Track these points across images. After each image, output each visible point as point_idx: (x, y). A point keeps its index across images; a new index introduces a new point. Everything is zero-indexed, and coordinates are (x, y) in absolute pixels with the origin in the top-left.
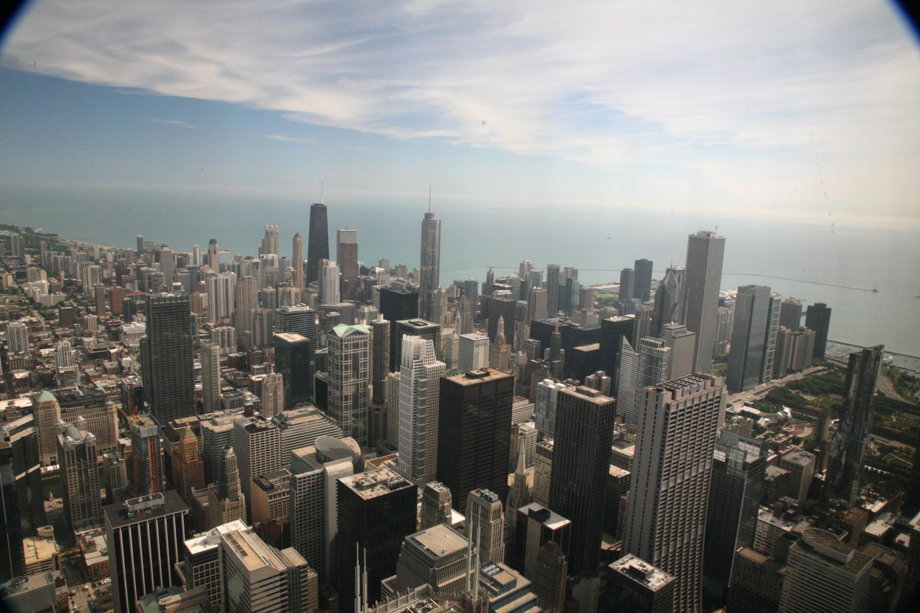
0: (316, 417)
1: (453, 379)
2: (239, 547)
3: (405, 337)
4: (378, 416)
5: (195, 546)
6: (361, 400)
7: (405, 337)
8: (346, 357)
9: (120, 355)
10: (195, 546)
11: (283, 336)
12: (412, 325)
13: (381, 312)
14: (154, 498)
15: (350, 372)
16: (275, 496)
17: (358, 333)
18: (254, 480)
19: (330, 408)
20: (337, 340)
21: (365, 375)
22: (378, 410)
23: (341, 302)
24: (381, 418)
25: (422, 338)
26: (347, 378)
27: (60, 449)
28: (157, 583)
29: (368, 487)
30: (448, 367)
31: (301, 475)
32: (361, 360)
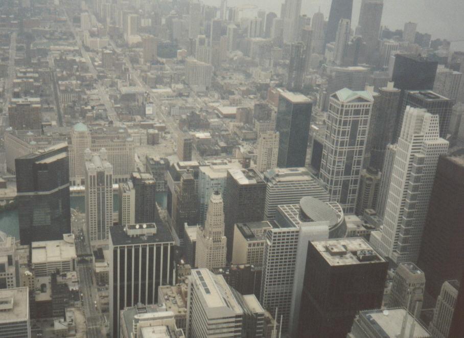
0: (306, 178)
1: (454, 159)
2: (204, 285)
3: (409, 110)
4: (369, 185)
7: (409, 110)
8: (345, 123)
12: (422, 96)
14: (148, 227)
15: (347, 138)
16: (254, 245)
17: (360, 99)
19: (322, 171)
20: (338, 105)
21: (362, 143)
22: (370, 179)
24: (373, 187)
25: (428, 111)
26: (342, 144)
28: (136, 302)
30: (452, 145)
31: (276, 230)
32: (361, 128)
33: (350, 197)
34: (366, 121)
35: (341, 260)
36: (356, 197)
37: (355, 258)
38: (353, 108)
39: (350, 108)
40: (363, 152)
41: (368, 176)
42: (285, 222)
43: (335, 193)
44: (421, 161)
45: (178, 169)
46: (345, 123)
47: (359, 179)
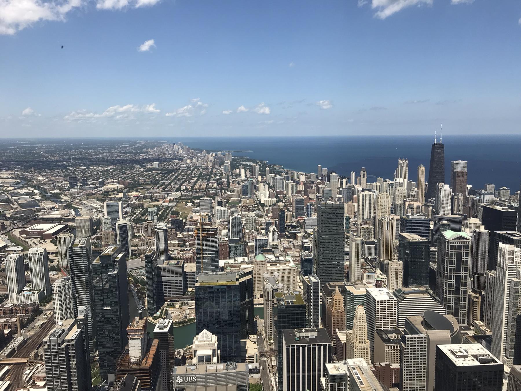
0: (426, 296)
5: (333, 368)
6: (462, 288)
9: (304, 237)
10: (333, 368)
11: (405, 235)
13: (483, 224)
15: (454, 266)
17: (461, 238)
18: (377, 332)
23: (452, 214)
27: (265, 290)
29: (460, 357)
32: (464, 259)
33: (461, 311)
34: (467, 255)
35: (464, 362)
36: (466, 311)
37: (475, 359)
38: (456, 244)
39: (454, 244)
40: (468, 277)
41: (474, 295)
42: (413, 330)
43: (449, 308)
44: (517, 284)
45: (329, 288)
46: (452, 255)
47: (467, 297)
